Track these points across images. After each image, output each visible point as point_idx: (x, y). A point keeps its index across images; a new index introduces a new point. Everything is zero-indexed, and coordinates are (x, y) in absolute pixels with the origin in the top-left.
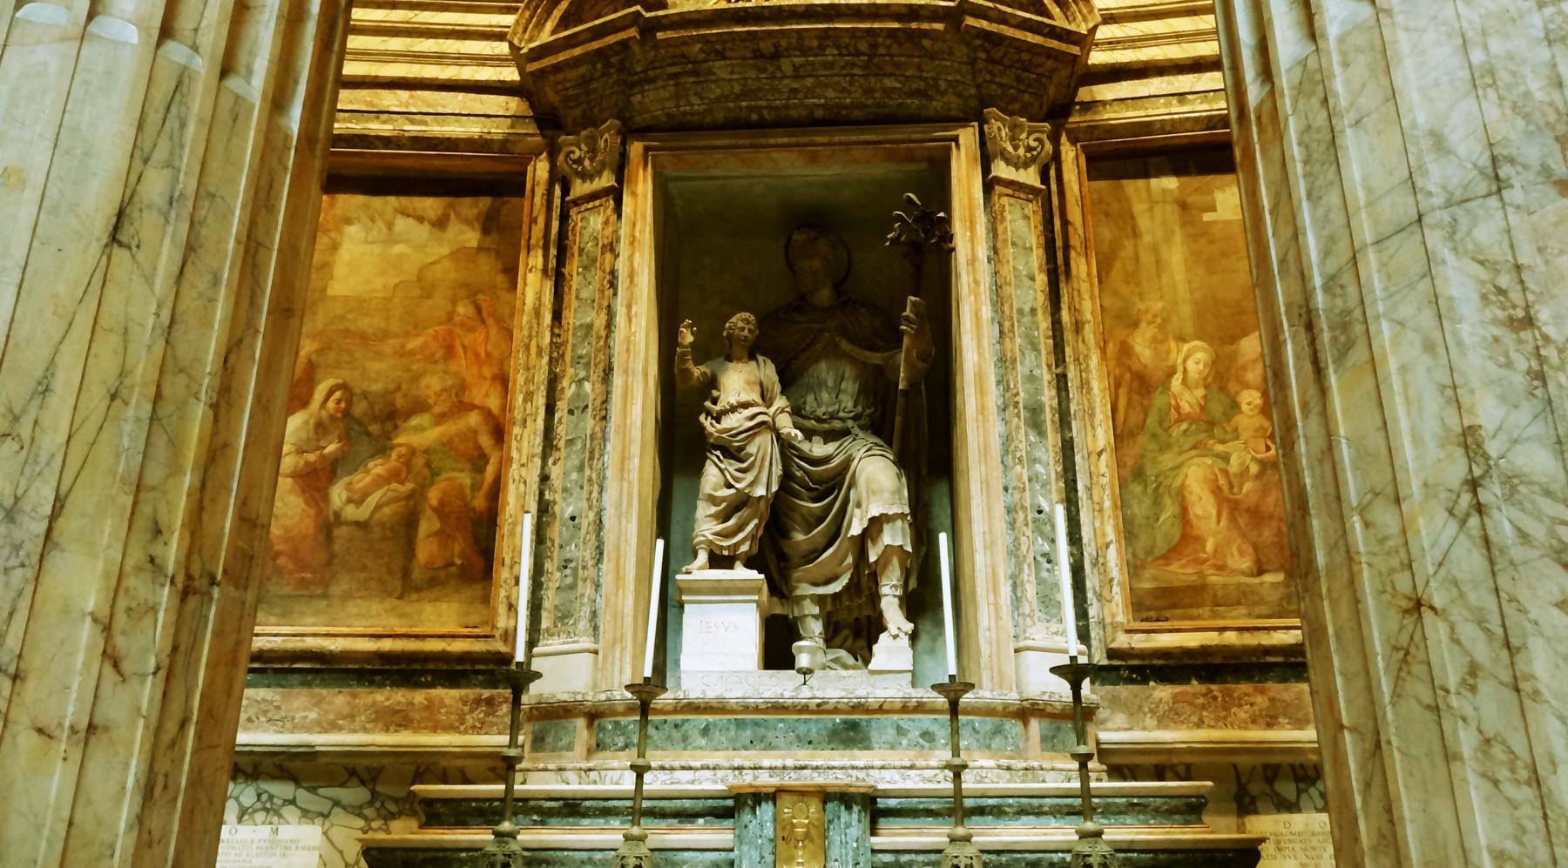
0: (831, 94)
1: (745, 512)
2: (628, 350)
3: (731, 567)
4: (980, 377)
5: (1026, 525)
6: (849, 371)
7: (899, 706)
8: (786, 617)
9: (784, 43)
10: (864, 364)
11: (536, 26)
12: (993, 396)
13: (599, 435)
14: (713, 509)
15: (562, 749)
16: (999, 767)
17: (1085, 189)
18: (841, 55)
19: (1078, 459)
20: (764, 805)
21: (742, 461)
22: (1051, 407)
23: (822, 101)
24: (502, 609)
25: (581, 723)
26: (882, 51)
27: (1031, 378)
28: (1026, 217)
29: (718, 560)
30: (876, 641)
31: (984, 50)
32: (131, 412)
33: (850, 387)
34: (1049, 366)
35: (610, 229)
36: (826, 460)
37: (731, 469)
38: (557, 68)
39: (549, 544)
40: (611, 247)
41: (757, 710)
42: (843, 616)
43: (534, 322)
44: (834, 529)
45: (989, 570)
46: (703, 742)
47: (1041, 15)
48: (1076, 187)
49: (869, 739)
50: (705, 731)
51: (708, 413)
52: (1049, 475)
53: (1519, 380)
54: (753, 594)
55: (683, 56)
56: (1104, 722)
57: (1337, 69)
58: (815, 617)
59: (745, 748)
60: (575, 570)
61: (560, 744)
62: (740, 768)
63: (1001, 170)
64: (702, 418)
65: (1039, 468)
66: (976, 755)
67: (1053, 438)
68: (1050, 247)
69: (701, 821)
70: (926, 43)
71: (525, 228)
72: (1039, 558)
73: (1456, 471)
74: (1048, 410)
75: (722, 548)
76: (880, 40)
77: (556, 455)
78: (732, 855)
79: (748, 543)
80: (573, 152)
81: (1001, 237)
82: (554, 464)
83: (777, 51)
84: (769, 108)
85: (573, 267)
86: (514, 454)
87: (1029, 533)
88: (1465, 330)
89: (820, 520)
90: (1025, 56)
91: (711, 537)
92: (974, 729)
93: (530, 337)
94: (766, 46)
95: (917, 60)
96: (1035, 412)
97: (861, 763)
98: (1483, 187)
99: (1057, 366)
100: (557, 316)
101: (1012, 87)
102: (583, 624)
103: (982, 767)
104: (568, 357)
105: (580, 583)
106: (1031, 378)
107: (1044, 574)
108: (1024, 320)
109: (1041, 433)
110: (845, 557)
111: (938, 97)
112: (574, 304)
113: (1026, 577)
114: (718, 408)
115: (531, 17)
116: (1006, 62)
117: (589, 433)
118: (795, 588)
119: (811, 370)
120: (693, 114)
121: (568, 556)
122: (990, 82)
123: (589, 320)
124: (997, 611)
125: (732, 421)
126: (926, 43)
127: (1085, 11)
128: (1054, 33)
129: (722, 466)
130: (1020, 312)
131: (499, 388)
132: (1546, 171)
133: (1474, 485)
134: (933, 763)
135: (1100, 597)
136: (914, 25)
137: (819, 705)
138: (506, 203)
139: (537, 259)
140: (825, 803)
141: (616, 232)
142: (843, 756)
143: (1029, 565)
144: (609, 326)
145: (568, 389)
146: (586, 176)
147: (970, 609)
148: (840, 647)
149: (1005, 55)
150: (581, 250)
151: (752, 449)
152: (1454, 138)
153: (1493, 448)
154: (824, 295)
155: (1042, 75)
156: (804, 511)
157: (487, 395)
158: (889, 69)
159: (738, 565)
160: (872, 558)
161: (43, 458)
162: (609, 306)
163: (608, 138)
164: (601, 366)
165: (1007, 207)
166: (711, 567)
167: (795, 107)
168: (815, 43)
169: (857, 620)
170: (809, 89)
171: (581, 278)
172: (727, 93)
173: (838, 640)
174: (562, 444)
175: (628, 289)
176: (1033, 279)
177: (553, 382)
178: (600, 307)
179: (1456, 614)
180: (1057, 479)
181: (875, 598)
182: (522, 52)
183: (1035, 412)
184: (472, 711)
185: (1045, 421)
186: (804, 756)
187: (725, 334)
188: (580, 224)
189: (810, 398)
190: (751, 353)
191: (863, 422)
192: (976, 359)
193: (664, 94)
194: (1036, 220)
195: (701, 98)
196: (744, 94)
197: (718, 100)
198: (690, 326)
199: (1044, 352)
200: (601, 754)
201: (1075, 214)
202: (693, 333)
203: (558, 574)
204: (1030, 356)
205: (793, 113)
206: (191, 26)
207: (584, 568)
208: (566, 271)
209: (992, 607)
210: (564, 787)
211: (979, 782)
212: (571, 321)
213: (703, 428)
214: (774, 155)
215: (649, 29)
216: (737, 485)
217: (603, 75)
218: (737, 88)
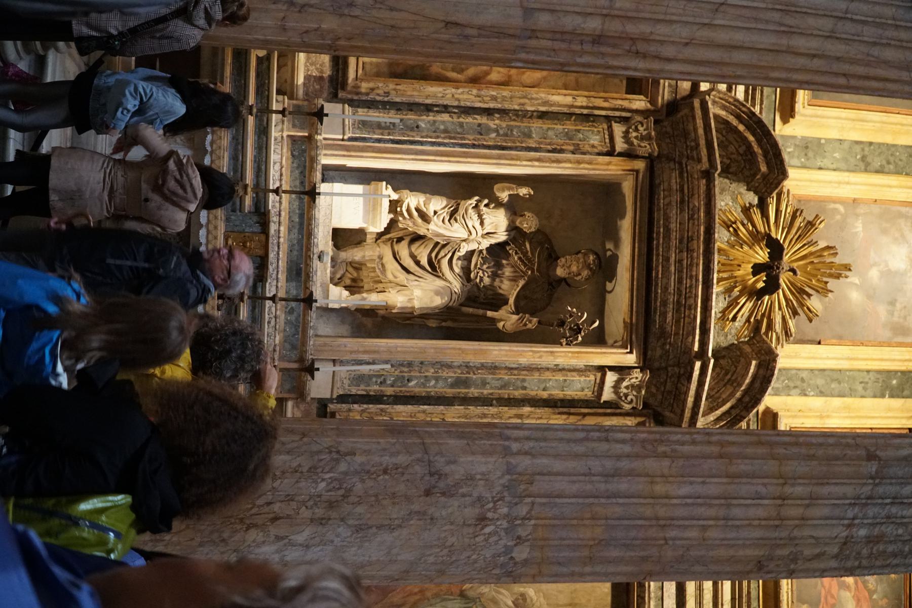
5: (401, 372)
15: (293, 122)
16: (275, 345)
20: (260, 228)
21: (449, 221)
22: (468, 393)
24: (371, 85)
28: (583, 390)
29: (394, 206)
32: (387, 31)
35: (590, 149)
41: (310, 224)
43: (540, 101)
49: (292, 281)
51: (479, 201)
52: (429, 387)
53: (368, 468)
56: (298, 407)
57: (490, 442)
59: (290, 218)
61: (296, 121)
62: (280, 215)
63: (611, 378)
65: (433, 383)
66: (282, 334)
67: (450, 392)
69: (254, 195)
70: (691, 338)
71: (602, 94)
72: (383, 377)
73: (342, 449)
74: (466, 391)
78: (238, 211)
80: (642, 126)
81: (569, 374)
86: (460, 90)
87: (397, 373)
88: (387, 458)
93: (532, 99)
96: (465, 383)
97: (280, 276)
98: (433, 470)
103: (275, 337)
104: (512, 123)
105: (381, 131)
106: (484, 383)
108: (519, 382)
109: (452, 386)
111: (659, 344)
112: (545, 127)
115: (729, 103)
116: (679, 385)
117: (465, 136)
120: (659, 199)
122: (667, 375)
123: (534, 136)
130: (524, 380)
131: (503, 79)
132: (434, 487)
133: (338, 452)
134: (278, 313)
135: (363, 411)
137: (310, 256)
138: (621, 81)
139: (582, 101)
140: (260, 257)
142: (283, 267)
146: (626, 133)
150: (578, 131)
152: (453, 467)
153: (348, 458)
157: (499, 72)
159: (392, 216)
161: (368, 11)
163: (645, 148)
167: (657, 260)
169: (362, 280)
171: (561, 131)
174: (461, 120)
175: (550, 159)
176: (544, 390)
177: (503, 112)
178: (540, 143)
179: (301, 443)
180: (427, 392)
182: (707, 97)
184: (317, 69)
185: (460, 388)
186: (284, 248)
188: (596, 130)
190: (512, 229)
195: (667, 205)
197: (665, 214)
199: (500, 392)
200: (290, 142)
204: (497, 384)
206: (539, 36)
210: (273, 124)
211: (268, 335)
212: (535, 125)
215: (708, 175)
217: (687, 146)
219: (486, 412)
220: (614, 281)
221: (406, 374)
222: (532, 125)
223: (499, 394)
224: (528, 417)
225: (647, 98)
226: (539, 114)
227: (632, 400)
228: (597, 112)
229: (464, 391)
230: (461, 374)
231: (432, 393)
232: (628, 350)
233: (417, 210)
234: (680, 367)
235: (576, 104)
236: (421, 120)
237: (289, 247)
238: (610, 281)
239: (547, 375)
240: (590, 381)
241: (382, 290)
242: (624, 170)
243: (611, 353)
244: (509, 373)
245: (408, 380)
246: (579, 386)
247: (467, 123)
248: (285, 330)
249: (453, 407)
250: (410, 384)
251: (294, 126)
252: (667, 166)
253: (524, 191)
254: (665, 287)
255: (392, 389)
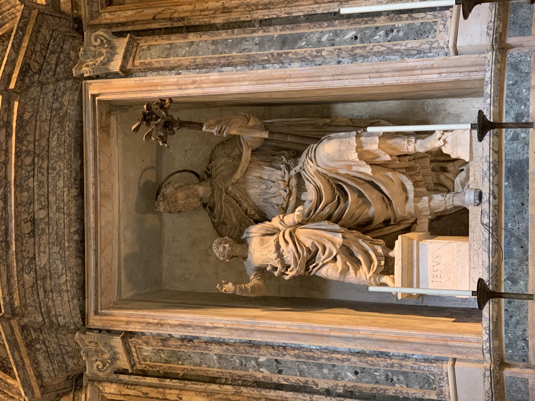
0: (60, 184)
1: (354, 249)
2: (235, 329)
3: (393, 259)
4: (259, 80)
5: (365, 47)
6: (255, 173)
7: (496, 139)
8: (431, 221)
9: (25, 216)
10: (250, 162)
11: (10, 390)
12: (274, 70)
13: (296, 352)
14: (352, 271)
15: (526, 387)
17: (132, 6)
18: (33, 176)
19: (319, 11)
21: (317, 250)
22: (281, 30)
23: (66, 189)
25: (507, 372)
26: (31, 147)
27: (261, 44)
30: (449, 156)
31: (33, 76)
33: (268, 172)
34: (254, 31)
36: (318, 190)
37: (323, 257)
38: (39, 376)
39: (375, 391)
40: (164, 340)
41: (497, 242)
42: (431, 180)
44: (367, 185)
45: (396, 74)
46: (522, 282)
47: (10, 36)
48: (130, 13)
49: (520, 161)
50: (514, 281)
52: (330, 31)
54: (412, 243)
55: (32, 287)
58: (430, 200)
60: (393, 373)
63: (116, 66)
64: (287, 278)
65: (324, 39)
67: (304, 29)
68: (170, 31)
72: (389, 38)
74: (283, 33)
75: (379, 265)
76: (24, 148)
77: (311, 384)
79: (376, 247)
80: (98, 366)
81: (162, 65)
82: (317, 385)
83: (30, 221)
84: (69, 227)
85: (178, 367)
87: (371, 46)
89: (361, 195)
90: (38, 48)
91: (371, 273)
92: (513, 85)
94: (27, 228)
95: (38, 123)
96: (284, 42)
99: (254, 27)
100: (213, 380)
101: (59, 57)
102: (434, 368)
105: (403, 369)
107: (401, 34)
109: (300, 37)
110: (388, 177)
111: (65, 109)
112: (204, 367)
113: (403, 47)
114: (279, 266)
116: (41, 61)
117: (295, 359)
118: (410, 213)
119: (255, 201)
120: (73, 281)
121: (383, 377)
123: (215, 357)
124: (427, 68)
125: (289, 257)
126: (27, 116)
127: (8, 7)
128: (22, 29)
129: (321, 264)
136: (14, 125)
137: (495, 198)
141: (154, 336)
143: (394, 45)
144: (220, 342)
145: (264, 374)
146: (114, 358)
147: (424, 87)
148: (454, 182)
149: (37, 62)
150: (166, 362)
151: (308, 244)
154: (202, 190)
155: (51, 36)
156: (354, 206)
158: (44, 143)
159: (391, 254)
160: (388, 158)
162: (206, 342)
164: (248, 349)
165: (142, 61)
166: (393, 274)
168: (25, 194)
169: (433, 170)
170: (57, 199)
171: (186, 362)
172: (59, 256)
173: (448, 184)
174: (303, 379)
175: (194, 329)
176: (192, 43)
178: (205, 349)
180: (333, 26)
181: (416, 157)
183: (284, 42)
185: (292, 35)
187: (227, 261)
188: (148, 362)
189: (274, 201)
191: (292, 164)
192: (247, 83)
193: (58, 302)
194: (152, 41)
195: (62, 275)
196: (60, 244)
198: (221, 286)
199: (243, 36)
201: (149, 12)
202: (227, 283)
203: (397, 385)
204: (246, 45)
205: (73, 211)
207: (392, 366)
208: (181, 373)
209: (424, 72)
212: (216, 370)
213: (294, 277)
214: (103, 223)
216: (334, 254)
217: (44, 343)
218: (56, 249)
219: (266, 12)
220: (143, 181)
221: (359, 45)
222: (220, 370)
223: (245, 33)
224: (216, 10)
225: (102, 396)
226: (217, 381)
227: (96, 41)
228: (155, 381)
229: (288, 32)
230: (288, 53)
231: (326, 24)
232: (97, 98)
233: (358, 263)
234: (39, 82)
235: (177, 392)
236: (352, 381)
237: (526, 211)
238: (147, 183)
239: (186, 61)
240: (140, 58)
241: (402, 158)
242: (111, 315)
243: (114, 93)
244: (230, 59)
245: (356, 38)
246: (153, 51)
247: (296, 375)
248: (529, 89)
249: (306, 13)
250: (354, 33)
251: (525, 382)
252: (67, 319)
253: (229, 287)
254: (60, 176)
255: (377, 25)
